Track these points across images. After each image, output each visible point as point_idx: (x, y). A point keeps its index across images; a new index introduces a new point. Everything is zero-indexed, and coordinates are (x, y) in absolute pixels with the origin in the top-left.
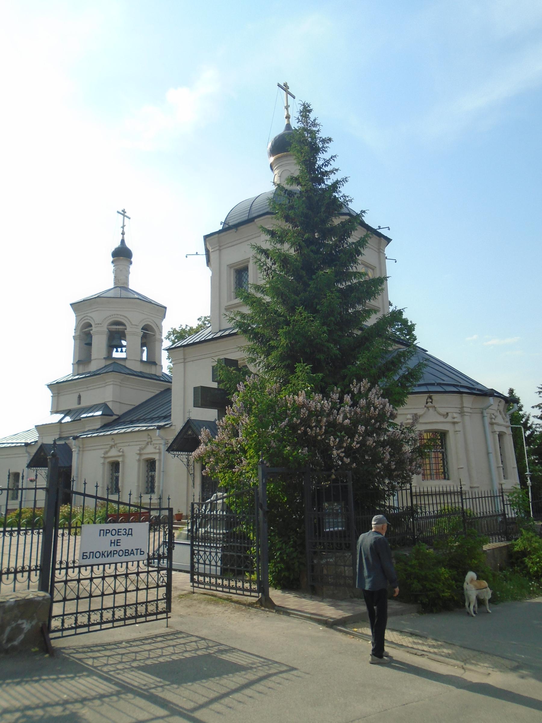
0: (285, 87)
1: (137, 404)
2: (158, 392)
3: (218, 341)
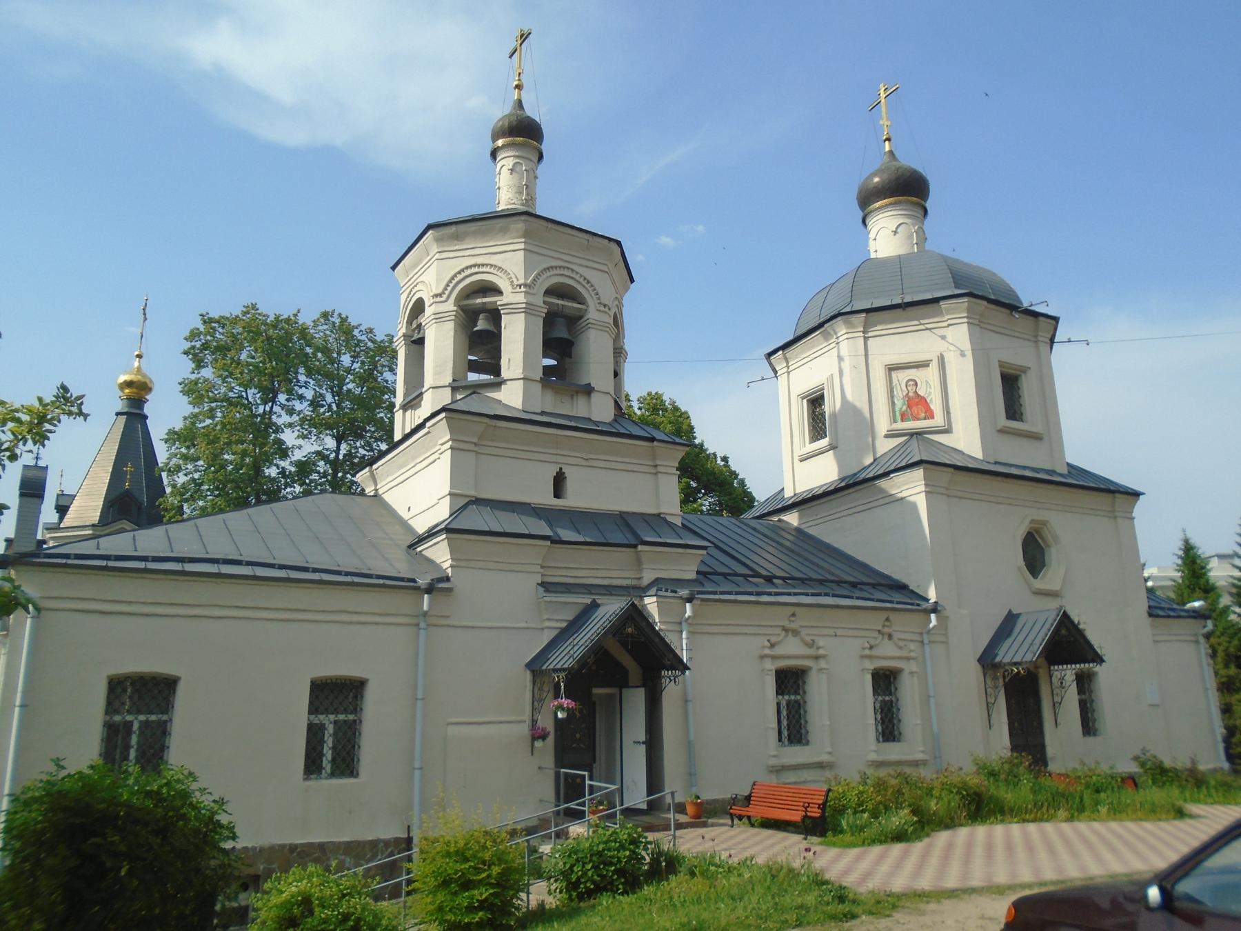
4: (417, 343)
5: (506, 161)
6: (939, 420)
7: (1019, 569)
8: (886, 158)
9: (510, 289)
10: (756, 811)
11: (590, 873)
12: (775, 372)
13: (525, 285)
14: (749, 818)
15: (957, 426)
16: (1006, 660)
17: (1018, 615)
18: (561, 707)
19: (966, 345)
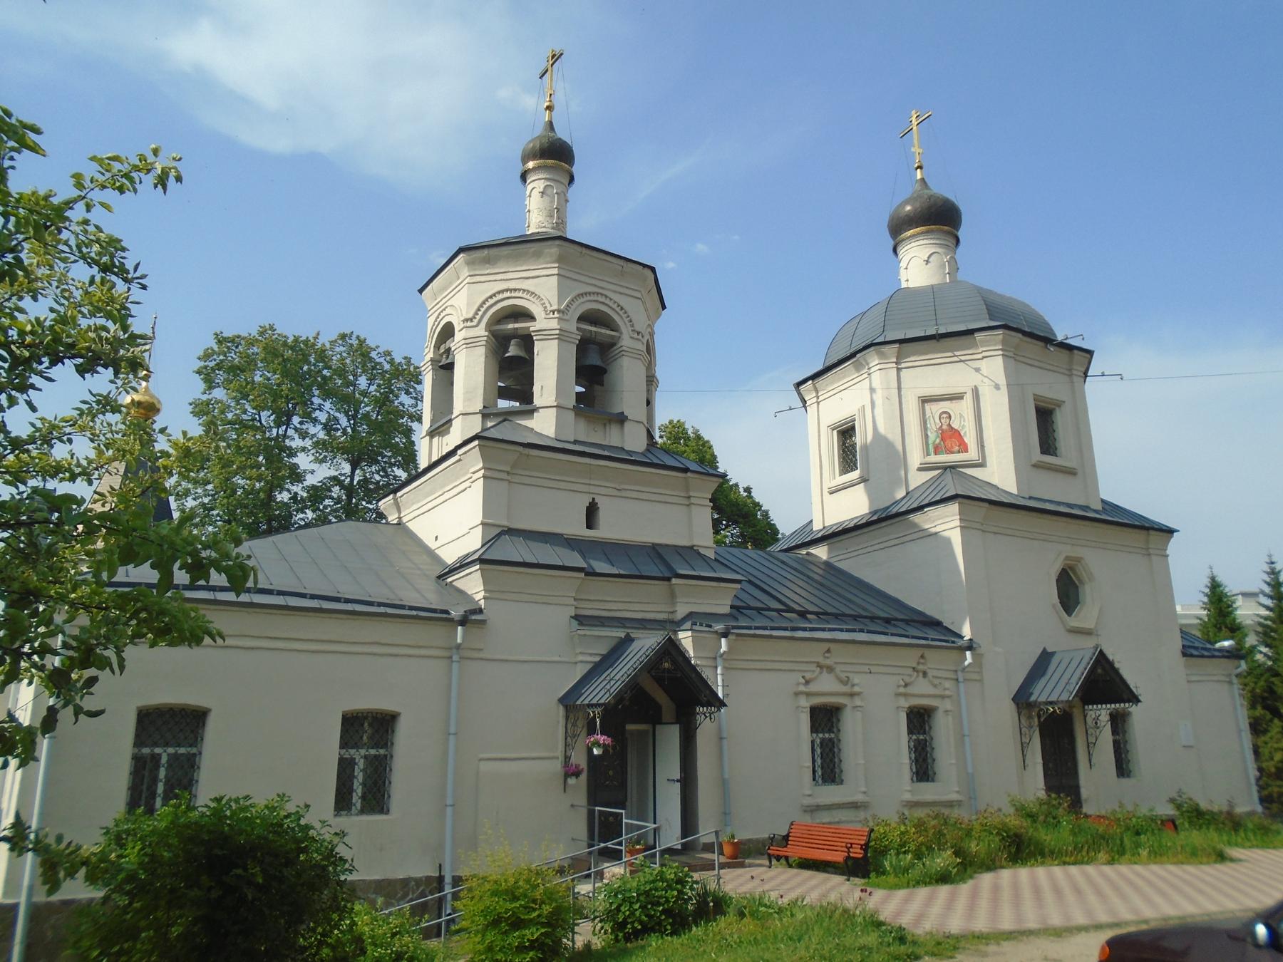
4: (445, 368)
5: (537, 184)
6: (972, 454)
7: (1054, 606)
8: (918, 187)
9: (543, 315)
10: (794, 851)
11: (638, 913)
12: (804, 402)
13: (559, 311)
14: (787, 858)
15: (991, 459)
16: (1042, 699)
17: (1053, 654)
18: (597, 744)
19: (1002, 381)
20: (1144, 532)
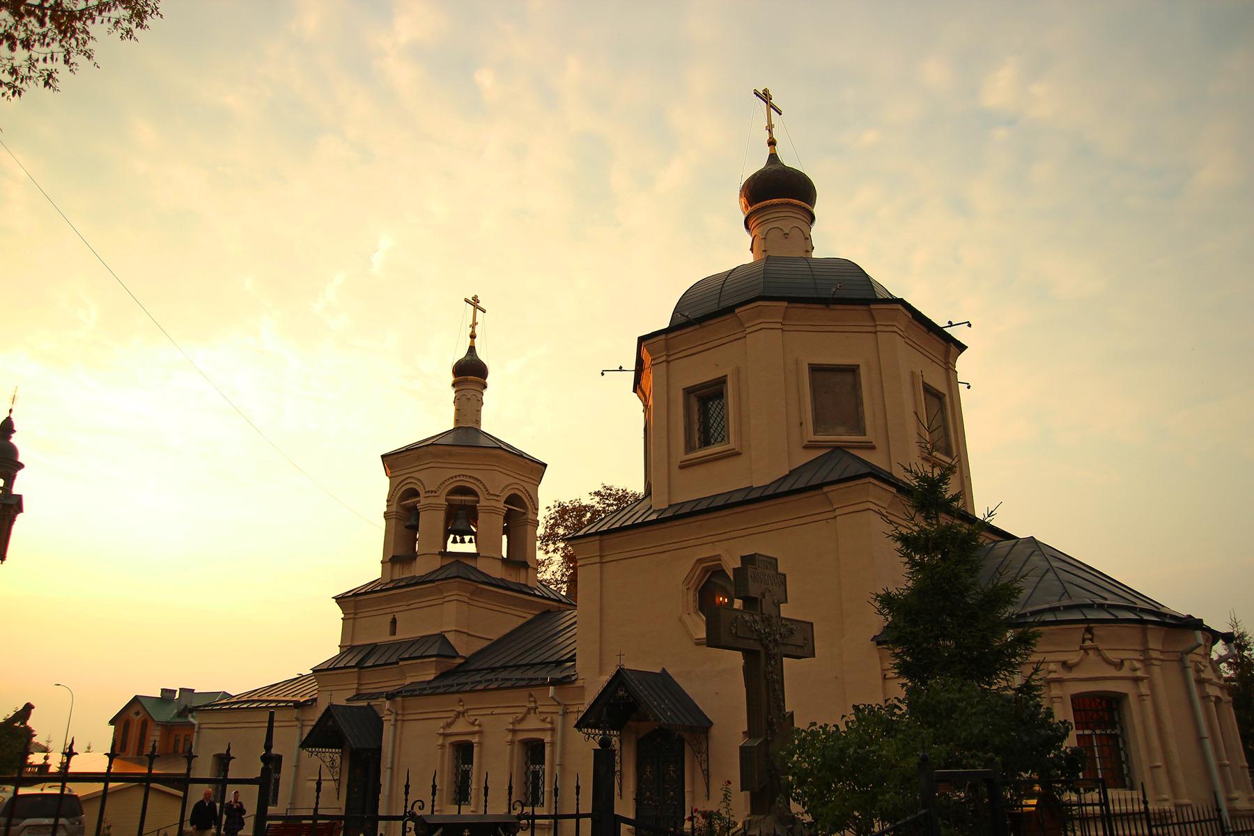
0: (765, 97)
1: (495, 637)
2: (530, 617)
3: (668, 524)
20: (819, 492)
